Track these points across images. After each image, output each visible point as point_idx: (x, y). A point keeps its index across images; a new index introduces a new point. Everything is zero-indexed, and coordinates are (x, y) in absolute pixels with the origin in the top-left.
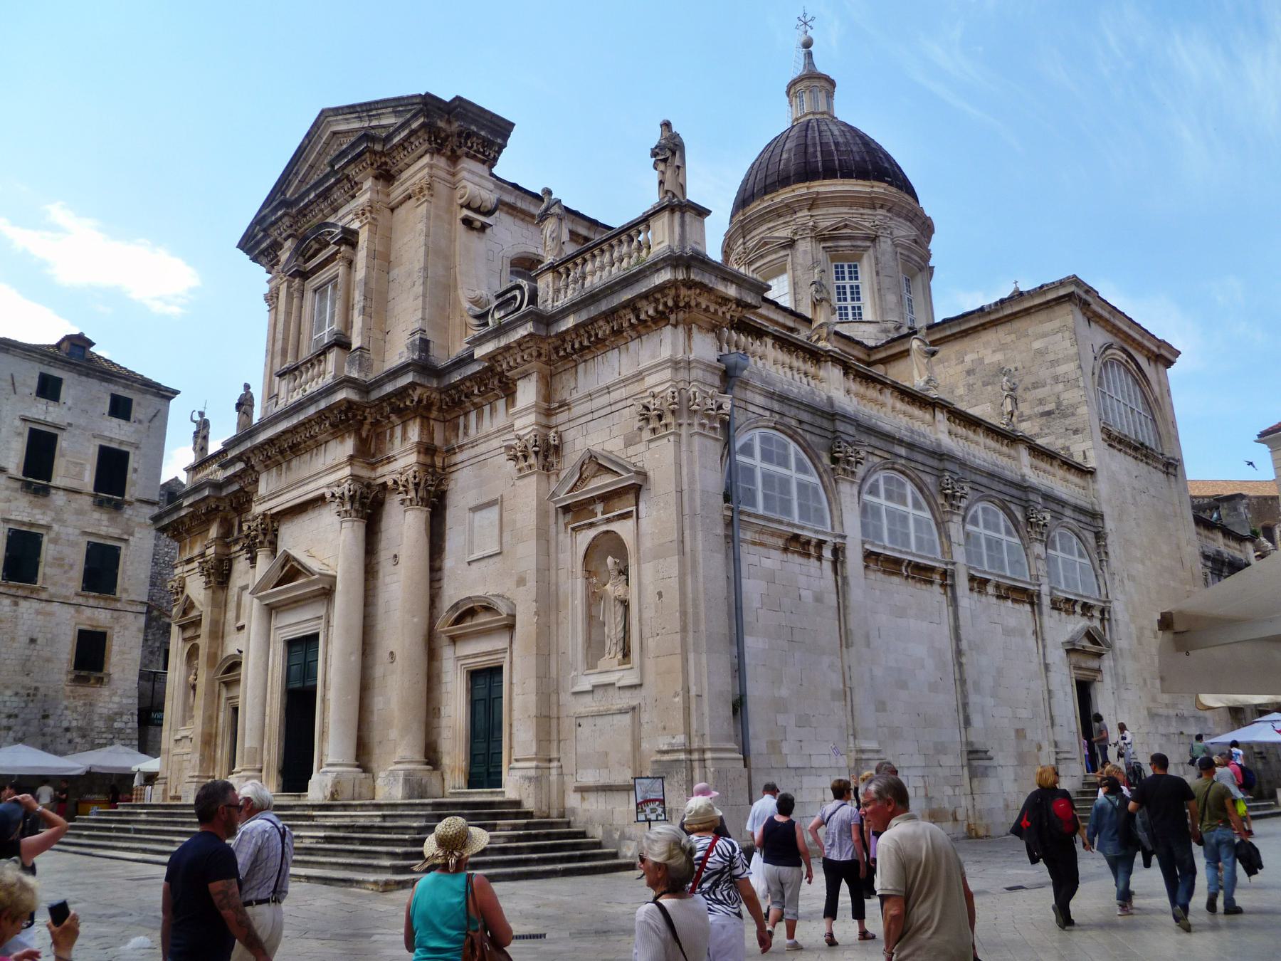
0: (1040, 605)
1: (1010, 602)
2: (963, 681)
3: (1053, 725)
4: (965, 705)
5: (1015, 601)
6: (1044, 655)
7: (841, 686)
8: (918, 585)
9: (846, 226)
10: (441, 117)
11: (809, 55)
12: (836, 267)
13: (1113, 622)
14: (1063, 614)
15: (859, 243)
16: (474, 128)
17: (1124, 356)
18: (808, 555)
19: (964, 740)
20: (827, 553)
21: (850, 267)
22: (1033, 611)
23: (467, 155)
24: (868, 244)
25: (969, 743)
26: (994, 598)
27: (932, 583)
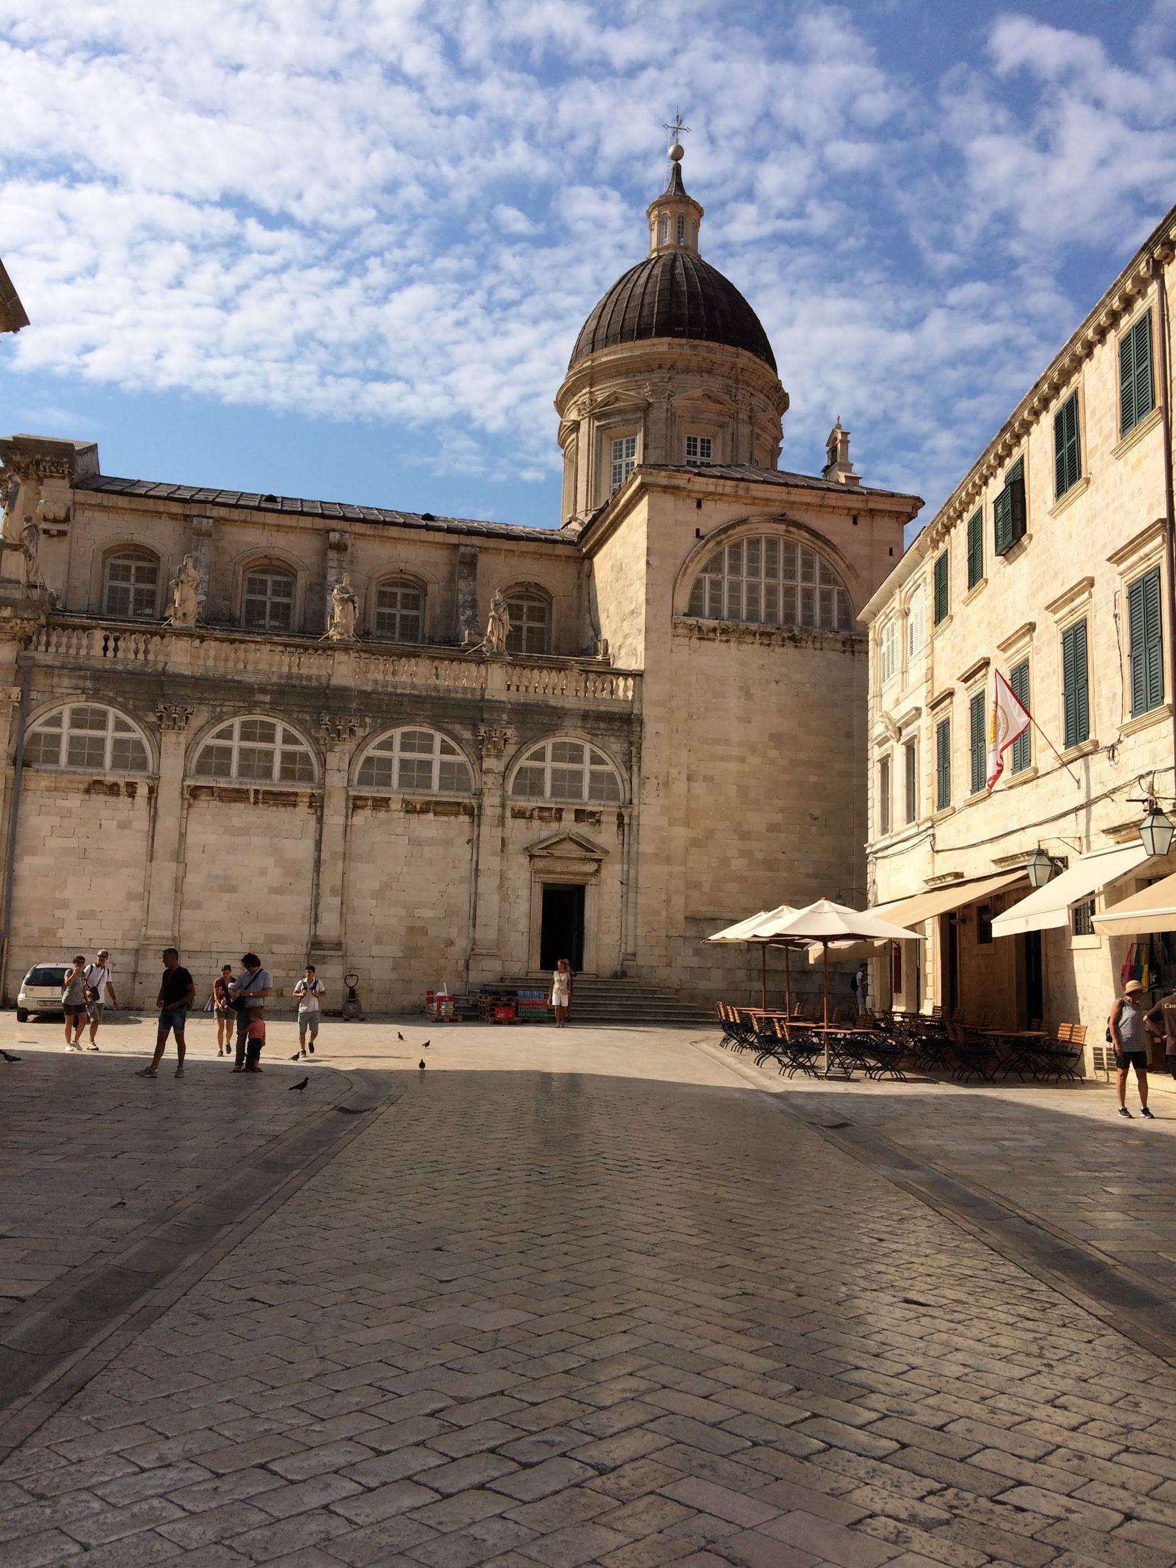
0: (479, 816)
1: (431, 816)
2: (318, 885)
3: (474, 926)
4: (317, 906)
5: (435, 814)
6: (477, 862)
7: (141, 890)
8: (274, 808)
9: (617, 399)
10: (14, 453)
12: (616, 444)
13: (635, 827)
14: (536, 823)
15: (629, 416)
16: (38, 457)
17: (783, 527)
18: (118, 795)
19: (312, 932)
20: (142, 791)
21: (628, 442)
22: (473, 822)
23: (46, 477)
24: (640, 414)
25: (315, 936)
26: (402, 814)
27: (295, 805)
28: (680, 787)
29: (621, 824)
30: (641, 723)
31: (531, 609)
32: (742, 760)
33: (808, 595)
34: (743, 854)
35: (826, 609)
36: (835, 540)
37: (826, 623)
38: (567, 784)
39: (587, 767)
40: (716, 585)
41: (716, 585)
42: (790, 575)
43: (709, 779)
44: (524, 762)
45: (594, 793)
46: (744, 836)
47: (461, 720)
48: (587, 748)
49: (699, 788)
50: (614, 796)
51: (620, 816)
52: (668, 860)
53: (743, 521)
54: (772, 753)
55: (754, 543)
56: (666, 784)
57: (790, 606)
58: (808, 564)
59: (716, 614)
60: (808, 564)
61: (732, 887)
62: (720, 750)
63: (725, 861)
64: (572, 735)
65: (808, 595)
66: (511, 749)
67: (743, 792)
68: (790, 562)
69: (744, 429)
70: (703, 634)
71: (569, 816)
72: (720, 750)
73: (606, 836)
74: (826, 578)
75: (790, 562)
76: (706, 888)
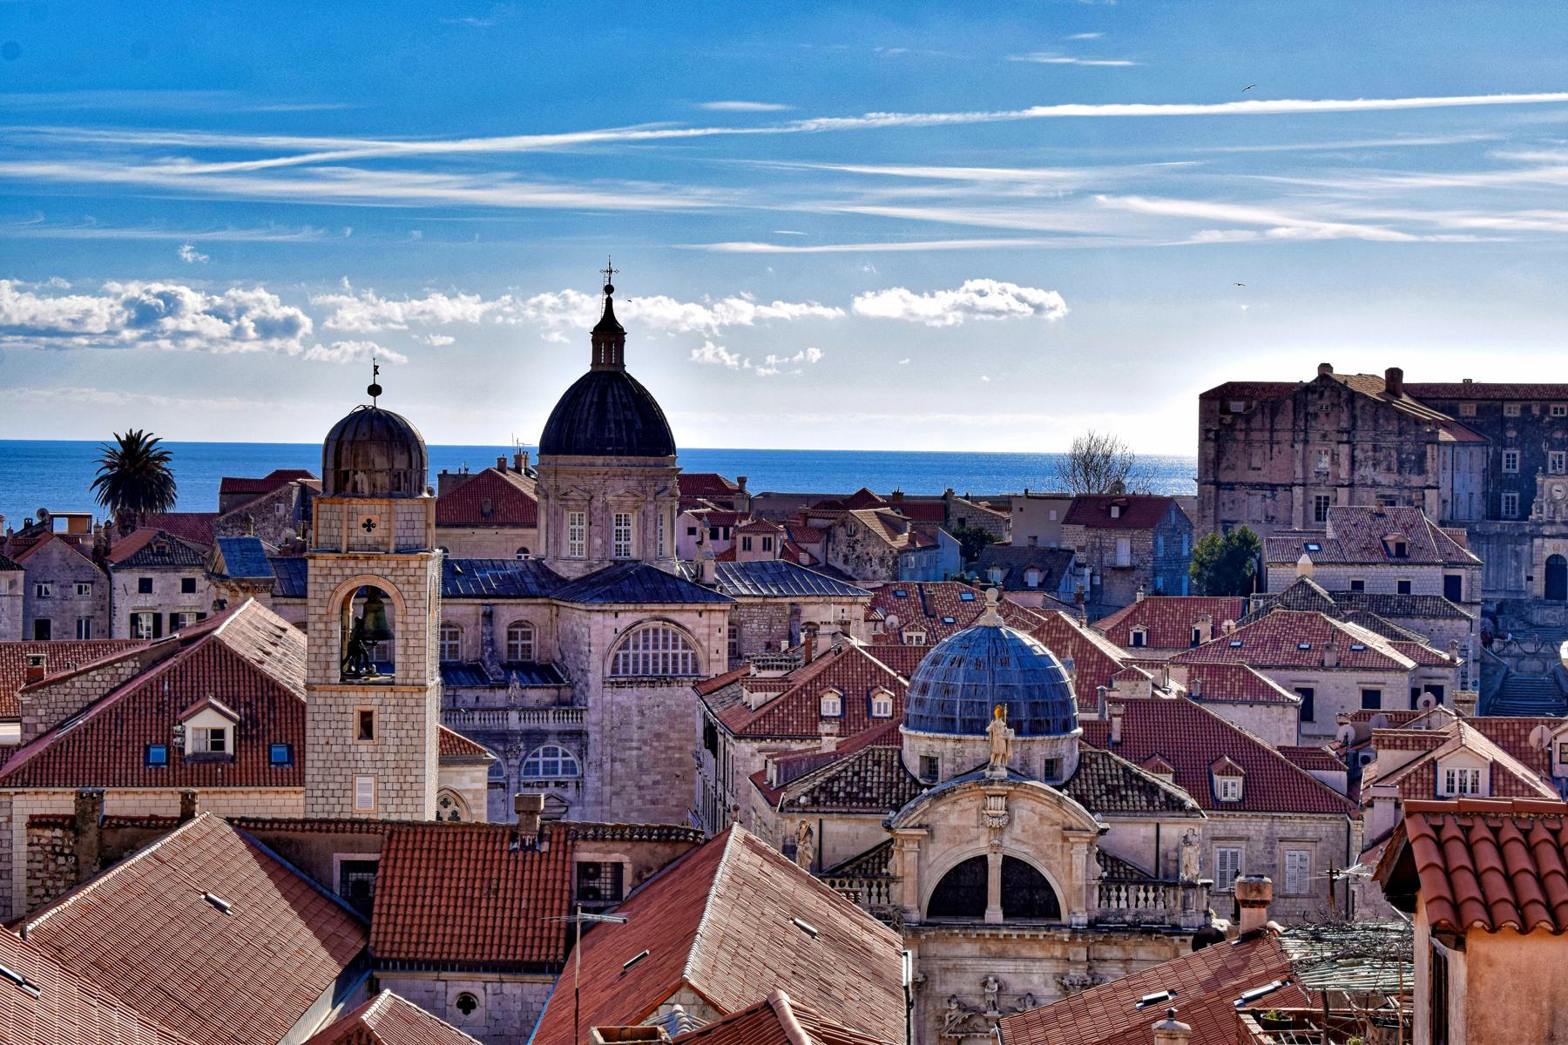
11: (609, 302)
28: (607, 766)
29: (578, 787)
30: (587, 734)
31: (523, 633)
32: (640, 749)
33: (675, 656)
34: (641, 797)
35: (685, 664)
36: (689, 626)
37: (685, 670)
38: (551, 768)
39: (560, 759)
40: (626, 656)
41: (626, 656)
42: (665, 647)
43: (622, 760)
44: (529, 759)
45: (564, 772)
46: (640, 788)
47: (496, 741)
48: (560, 749)
49: (617, 765)
50: (574, 772)
51: (577, 783)
52: (601, 803)
53: (640, 622)
54: (655, 744)
55: (646, 632)
56: (601, 765)
57: (666, 664)
58: (675, 640)
59: (625, 671)
60: (675, 640)
61: (635, 814)
62: (628, 744)
63: (631, 802)
64: (552, 743)
65: (675, 656)
66: (523, 753)
67: (640, 766)
68: (665, 639)
69: (651, 507)
70: (619, 685)
71: (552, 785)
72: (628, 744)
73: (570, 794)
74: (685, 647)
75: (665, 639)
76: (621, 816)
